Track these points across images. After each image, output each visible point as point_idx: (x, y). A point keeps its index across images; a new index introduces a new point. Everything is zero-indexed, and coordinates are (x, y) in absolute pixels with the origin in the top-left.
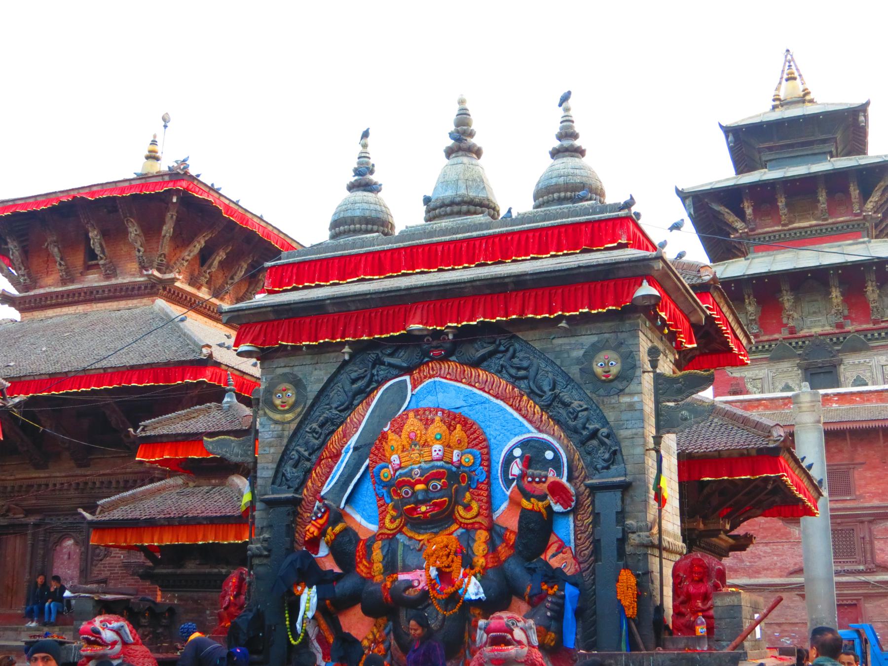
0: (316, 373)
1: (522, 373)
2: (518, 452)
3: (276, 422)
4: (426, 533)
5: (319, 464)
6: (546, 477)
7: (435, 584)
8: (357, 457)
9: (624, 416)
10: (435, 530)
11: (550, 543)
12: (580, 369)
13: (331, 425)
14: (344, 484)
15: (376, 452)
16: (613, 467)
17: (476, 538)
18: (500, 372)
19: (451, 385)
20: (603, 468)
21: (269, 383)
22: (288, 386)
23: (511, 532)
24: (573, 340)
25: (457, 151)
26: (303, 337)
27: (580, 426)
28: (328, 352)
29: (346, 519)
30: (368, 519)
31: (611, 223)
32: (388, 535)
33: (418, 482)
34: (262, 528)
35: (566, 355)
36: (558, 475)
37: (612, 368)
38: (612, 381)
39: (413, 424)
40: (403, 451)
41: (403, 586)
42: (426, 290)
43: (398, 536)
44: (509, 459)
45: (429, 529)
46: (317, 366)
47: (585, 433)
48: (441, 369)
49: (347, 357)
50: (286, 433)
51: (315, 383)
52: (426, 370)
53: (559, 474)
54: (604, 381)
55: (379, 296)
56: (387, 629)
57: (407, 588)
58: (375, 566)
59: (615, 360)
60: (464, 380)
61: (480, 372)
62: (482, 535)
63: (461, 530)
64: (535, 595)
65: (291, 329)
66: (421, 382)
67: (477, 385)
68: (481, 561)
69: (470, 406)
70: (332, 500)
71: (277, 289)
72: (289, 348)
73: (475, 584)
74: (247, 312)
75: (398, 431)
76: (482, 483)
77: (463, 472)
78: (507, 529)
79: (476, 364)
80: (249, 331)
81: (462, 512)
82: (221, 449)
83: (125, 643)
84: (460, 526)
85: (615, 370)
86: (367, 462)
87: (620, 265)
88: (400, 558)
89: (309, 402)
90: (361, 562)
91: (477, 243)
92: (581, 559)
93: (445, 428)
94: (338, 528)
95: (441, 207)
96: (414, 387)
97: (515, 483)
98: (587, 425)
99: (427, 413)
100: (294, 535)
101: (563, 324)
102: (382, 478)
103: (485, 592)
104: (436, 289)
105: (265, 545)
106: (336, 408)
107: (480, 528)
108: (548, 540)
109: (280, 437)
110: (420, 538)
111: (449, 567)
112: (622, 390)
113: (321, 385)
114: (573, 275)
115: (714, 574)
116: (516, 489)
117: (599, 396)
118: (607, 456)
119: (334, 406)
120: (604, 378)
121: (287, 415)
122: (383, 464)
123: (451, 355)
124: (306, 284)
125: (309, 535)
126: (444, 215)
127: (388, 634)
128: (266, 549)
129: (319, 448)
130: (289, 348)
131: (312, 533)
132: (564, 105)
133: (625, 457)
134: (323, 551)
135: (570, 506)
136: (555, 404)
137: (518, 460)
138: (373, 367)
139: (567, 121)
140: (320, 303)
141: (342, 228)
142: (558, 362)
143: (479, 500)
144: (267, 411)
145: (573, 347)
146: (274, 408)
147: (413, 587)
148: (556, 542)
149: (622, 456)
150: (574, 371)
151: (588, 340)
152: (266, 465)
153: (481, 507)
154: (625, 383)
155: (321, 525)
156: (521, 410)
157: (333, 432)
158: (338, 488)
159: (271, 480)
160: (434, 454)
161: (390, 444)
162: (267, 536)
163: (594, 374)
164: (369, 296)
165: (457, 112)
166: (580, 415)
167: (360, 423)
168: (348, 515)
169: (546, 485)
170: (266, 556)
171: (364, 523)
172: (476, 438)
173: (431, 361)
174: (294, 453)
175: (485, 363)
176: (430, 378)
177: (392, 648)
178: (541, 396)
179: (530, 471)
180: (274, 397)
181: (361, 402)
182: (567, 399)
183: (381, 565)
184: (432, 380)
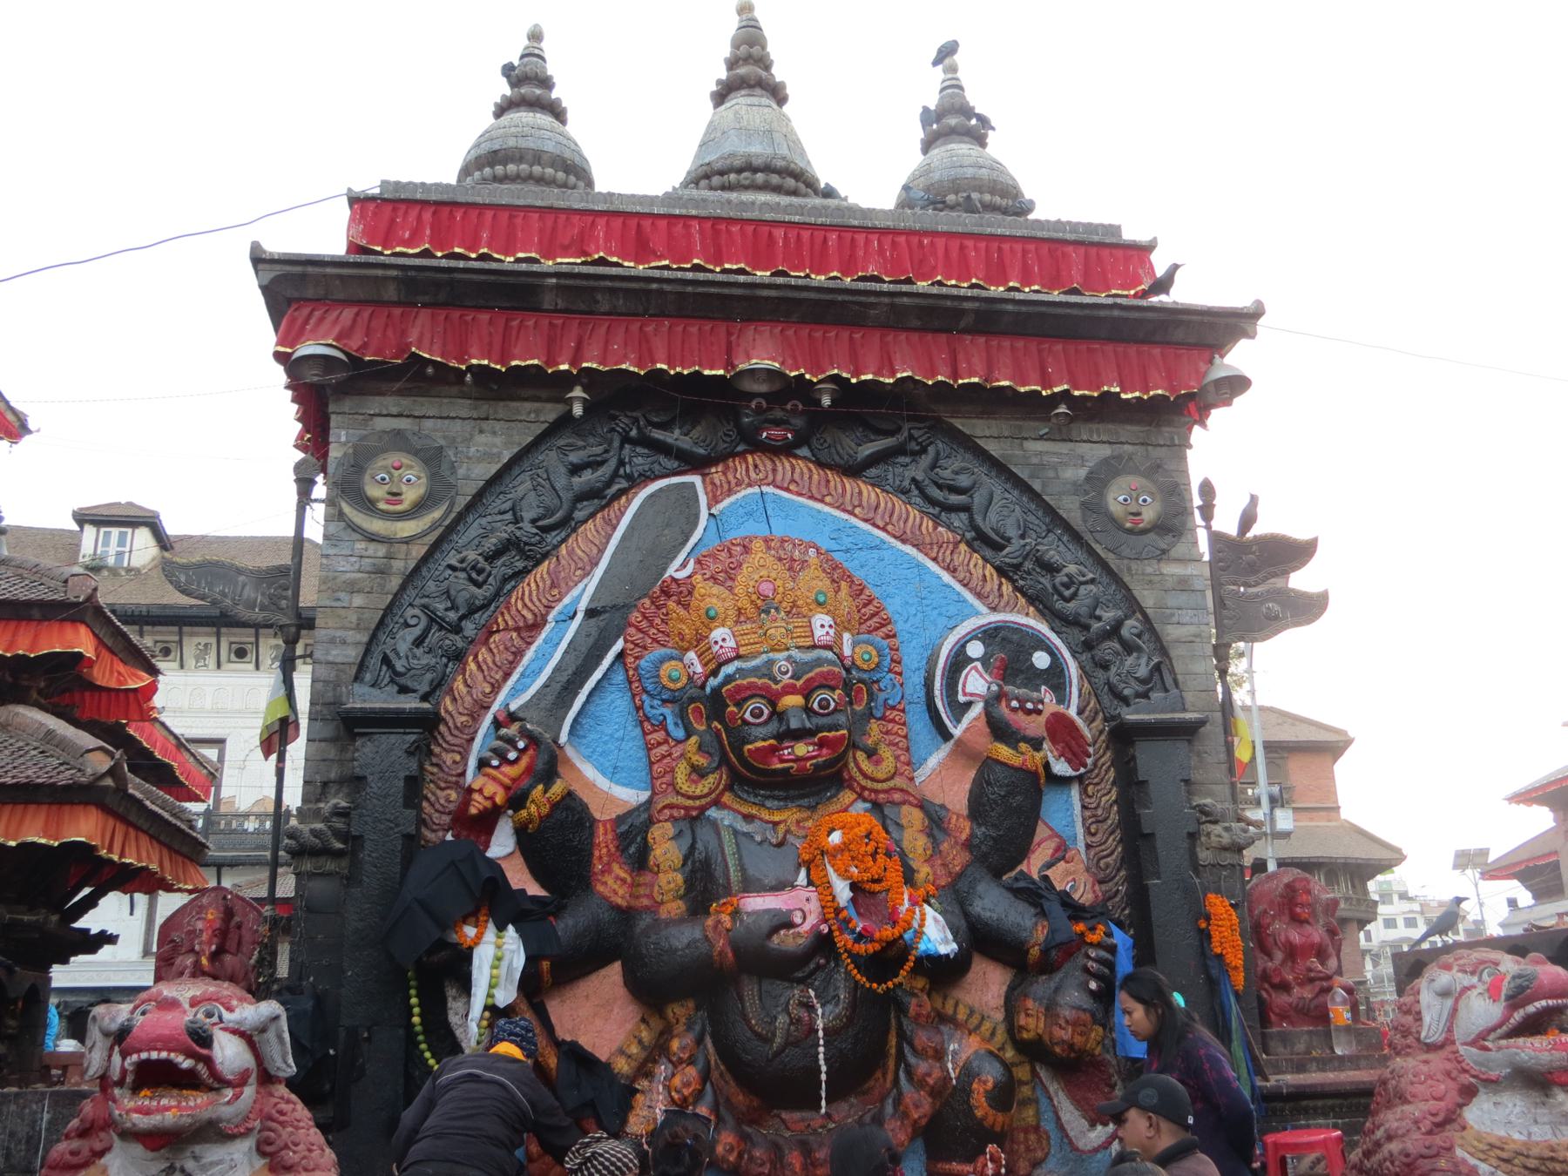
0: (481, 438)
1: (955, 499)
2: (976, 649)
3: (372, 538)
4: (786, 807)
5: (486, 642)
6: (1042, 702)
7: (848, 921)
8: (594, 632)
9: (1173, 600)
10: (805, 802)
11: (1037, 839)
12: (1083, 504)
13: (524, 553)
14: (565, 688)
15: (644, 624)
16: (1156, 696)
17: (904, 822)
18: (905, 492)
19: (803, 506)
20: (1138, 695)
21: (355, 447)
22: (405, 459)
23: (958, 816)
24: (1063, 448)
25: (751, 87)
26: (473, 350)
27: (1084, 610)
28: (513, 399)
29: (561, 770)
30: (613, 773)
31: (1119, 253)
32: (686, 808)
33: (790, 690)
34: (325, 784)
35: (1051, 474)
36: (1060, 701)
37: (1144, 510)
38: (1144, 532)
39: (758, 570)
40: (737, 622)
41: (765, 924)
42: (790, 294)
43: (713, 813)
44: (959, 661)
45: (792, 799)
46: (484, 425)
47: (1096, 625)
48: (774, 470)
49: (578, 410)
50: (398, 565)
51: (479, 460)
52: (741, 469)
53: (1062, 699)
54: (1130, 532)
55: (679, 288)
56: (698, 1028)
57: (775, 930)
58: (663, 879)
59: (1151, 494)
60: (828, 499)
61: (863, 486)
62: (913, 817)
63: (861, 806)
64: (1059, 945)
65: (440, 329)
66: (730, 492)
67: (857, 511)
68: (923, 871)
69: (847, 551)
70: (539, 724)
71: (379, 249)
72: (430, 370)
73: (935, 920)
74: (329, 270)
75: (726, 578)
76: (893, 708)
77: (860, 681)
78: (943, 806)
79: (853, 470)
80: (321, 320)
81: (866, 765)
82: (210, 585)
83: (266, 1078)
84: (860, 797)
85: (1149, 515)
86: (619, 645)
87: (1185, 317)
88: (731, 862)
89: (462, 502)
90: (607, 870)
91: (860, 238)
92: (1102, 875)
93: (828, 582)
94: (557, 788)
95: (739, 171)
96: (714, 500)
97: (977, 709)
98: (1098, 612)
99: (789, 547)
100: (420, 809)
101: (1062, 409)
102: (665, 681)
103: (955, 940)
104: (813, 295)
105: (339, 824)
106: (533, 521)
107: (904, 803)
108: (1032, 832)
109: (381, 572)
110: (777, 819)
111: (878, 881)
112: (1164, 552)
113: (499, 466)
114: (1099, 319)
115: (1319, 909)
116: (982, 723)
117: (1122, 558)
118: (1143, 671)
119: (528, 515)
120: (1128, 525)
121: (400, 525)
122: (663, 651)
123: (798, 446)
124: (457, 250)
125: (477, 805)
126: (746, 188)
127: (699, 1041)
128: (337, 834)
129: (484, 607)
130: (430, 370)
131: (491, 798)
132: (947, 61)
133: (1180, 677)
134: (502, 845)
135: (1085, 766)
136: (1028, 565)
137: (978, 664)
138: (622, 447)
139: (953, 87)
140: (530, 280)
141: (512, 168)
142: (1037, 486)
143: (891, 744)
144: (347, 509)
145: (1065, 464)
146: (369, 505)
147: (790, 925)
148: (1050, 837)
149: (1172, 671)
150: (1070, 508)
151: (1096, 453)
152: (339, 633)
153: (897, 758)
154: (1169, 538)
155: (514, 780)
156: (955, 570)
157: (525, 572)
158: (550, 698)
159: (354, 670)
160: (819, 632)
161: (694, 603)
162: (344, 804)
163: (1113, 519)
164: (654, 286)
165: (736, 26)
166: (1083, 590)
167: (595, 563)
168: (568, 761)
169: (1042, 719)
170: (338, 854)
171: (603, 783)
172: (869, 616)
173: (752, 453)
174: (417, 611)
175: (873, 472)
176: (750, 485)
177: (715, 1075)
178: (998, 547)
179: (1008, 688)
180: (367, 477)
181: (592, 515)
182: (1053, 556)
183: (679, 878)
184: (756, 489)
